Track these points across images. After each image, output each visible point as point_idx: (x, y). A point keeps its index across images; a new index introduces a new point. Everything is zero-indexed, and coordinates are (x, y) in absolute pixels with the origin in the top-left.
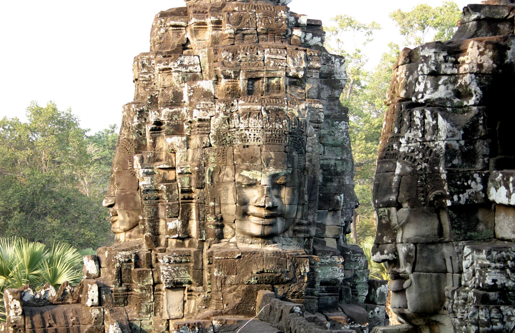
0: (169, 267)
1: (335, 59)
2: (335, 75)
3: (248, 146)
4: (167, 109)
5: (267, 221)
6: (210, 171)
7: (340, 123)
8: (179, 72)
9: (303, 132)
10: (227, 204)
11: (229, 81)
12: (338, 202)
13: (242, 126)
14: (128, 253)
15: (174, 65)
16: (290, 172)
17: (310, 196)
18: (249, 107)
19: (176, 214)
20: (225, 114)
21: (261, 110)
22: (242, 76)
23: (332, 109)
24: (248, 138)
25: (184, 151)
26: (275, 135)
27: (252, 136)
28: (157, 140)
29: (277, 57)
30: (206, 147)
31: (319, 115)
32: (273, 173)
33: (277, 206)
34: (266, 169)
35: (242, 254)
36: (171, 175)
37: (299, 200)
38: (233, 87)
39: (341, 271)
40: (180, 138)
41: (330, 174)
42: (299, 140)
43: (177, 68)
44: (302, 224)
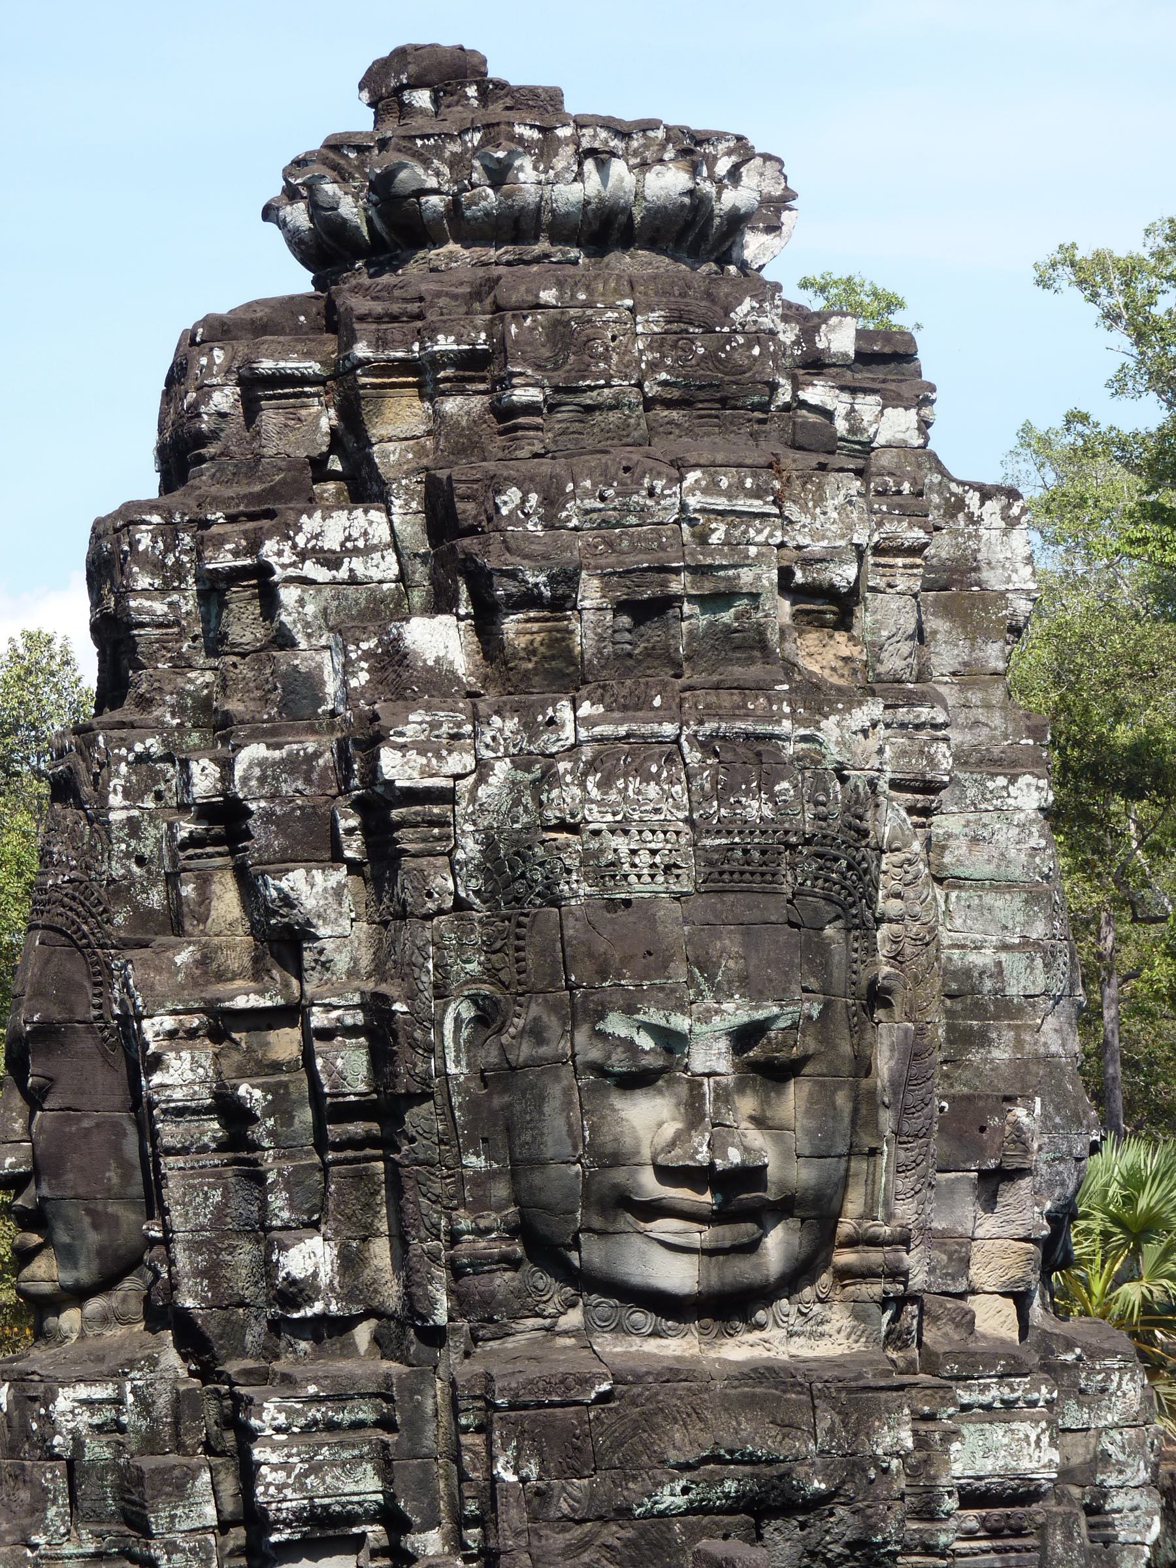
1: (982, 504)
3: (627, 903)
5: (726, 1234)
6: (458, 1020)
10: (543, 1163)
11: (528, 620)
12: (1019, 1137)
13: (598, 818)
14: (100, 1392)
15: (280, 553)
18: (622, 730)
19: (310, 1212)
20: (522, 762)
21: (677, 741)
23: (977, 723)
24: (626, 867)
25: (339, 930)
26: (746, 852)
28: (216, 888)
30: (440, 912)
32: (743, 1017)
33: (766, 1166)
34: (710, 1003)
35: (616, 1382)
37: (854, 1132)
38: (552, 643)
39: (1045, 1439)
41: (978, 1011)
42: (850, 867)
43: (293, 565)
44: (874, 1242)
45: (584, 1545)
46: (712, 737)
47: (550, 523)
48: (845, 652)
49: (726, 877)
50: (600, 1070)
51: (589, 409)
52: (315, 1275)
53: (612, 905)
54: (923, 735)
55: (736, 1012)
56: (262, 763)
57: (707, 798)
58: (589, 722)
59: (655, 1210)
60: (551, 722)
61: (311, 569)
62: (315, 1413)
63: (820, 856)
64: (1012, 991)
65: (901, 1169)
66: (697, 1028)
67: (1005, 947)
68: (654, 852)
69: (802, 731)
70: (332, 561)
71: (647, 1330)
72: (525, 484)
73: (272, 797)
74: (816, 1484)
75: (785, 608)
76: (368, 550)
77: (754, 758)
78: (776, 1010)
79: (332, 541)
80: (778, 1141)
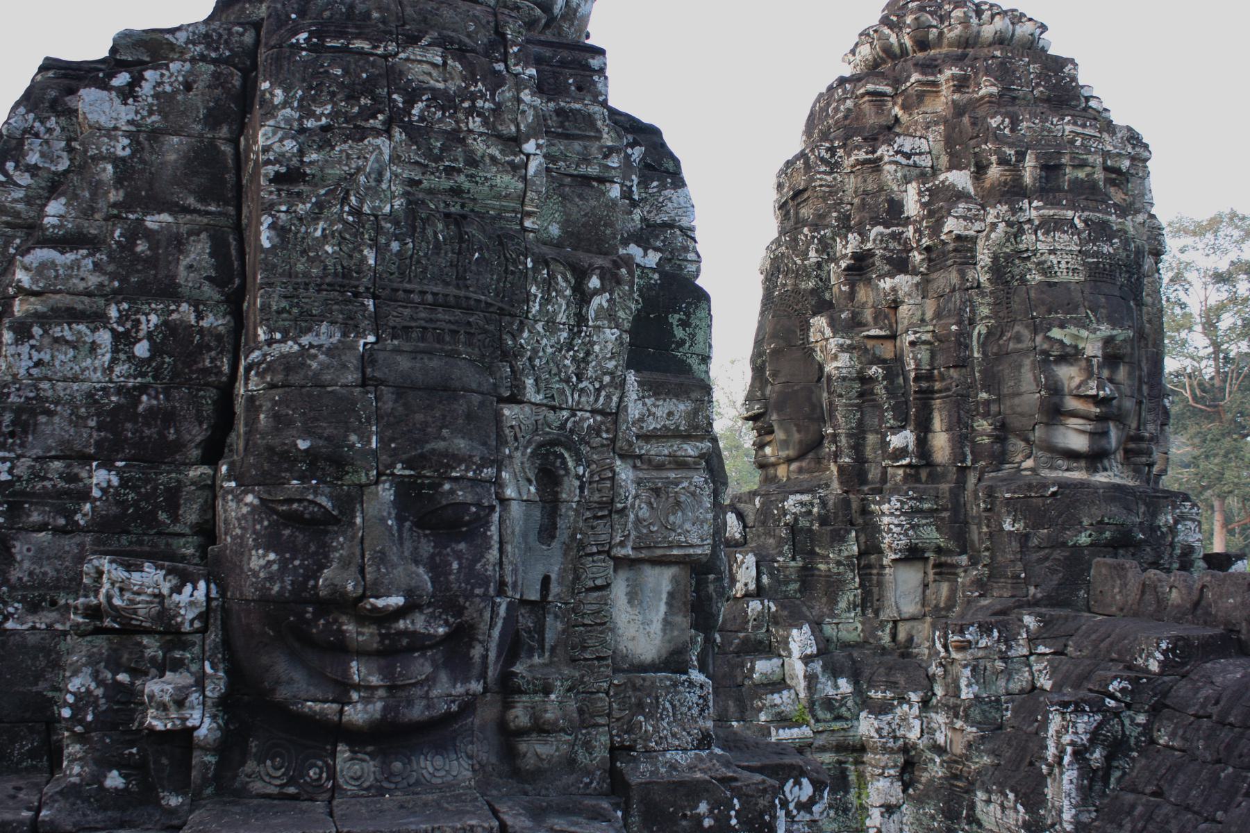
0: (902, 518)
4: (880, 229)
6: (979, 334)
8: (897, 163)
13: (1042, 247)
18: (1052, 212)
20: (1009, 224)
22: (1030, 161)
27: (1063, 265)
29: (1087, 131)
30: (972, 288)
32: (1108, 333)
36: (887, 351)
40: (908, 277)
45: (1046, 558)
47: (1012, 130)
50: (1046, 353)
51: (1014, 98)
53: (1050, 285)
55: (1105, 330)
56: (881, 234)
57: (1088, 243)
58: (1037, 208)
59: (1074, 414)
62: (911, 503)
65: (1150, 411)
70: (908, 156)
72: (1005, 115)
73: (885, 249)
76: (921, 154)
77: (1101, 231)
79: (907, 149)
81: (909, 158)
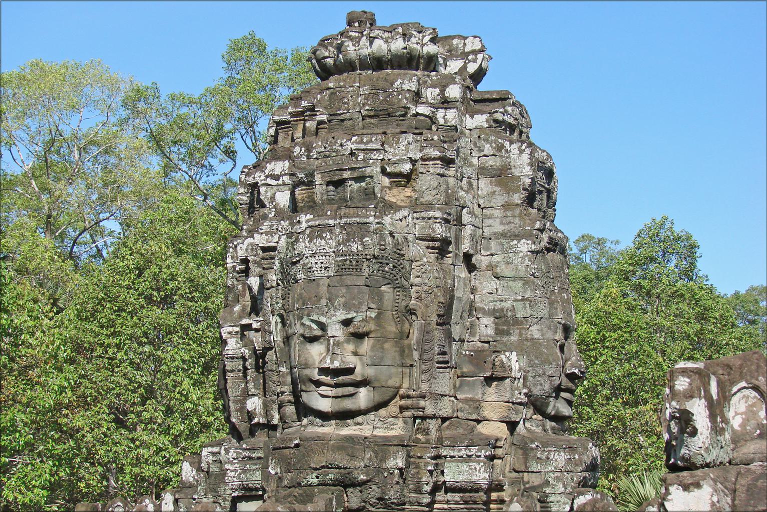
2: (513, 170)
3: (314, 280)
7: (518, 242)
9: (403, 255)
11: (304, 190)
15: (260, 177)
16: (373, 315)
17: (422, 352)
18: (317, 223)
26: (351, 262)
30: (272, 287)
31: (433, 229)
32: (343, 317)
34: (332, 312)
38: (309, 197)
39: (482, 469)
41: (506, 323)
43: (264, 180)
46: (346, 224)
47: (309, 157)
48: (409, 194)
49: (344, 270)
51: (342, 121)
52: (255, 409)
54: (431, 221)
55: (341, 315)
59: (318, 384)
60: (299, 222)
61: (269, 181)
62: (247, 454)
63: (381, 263)
64: (518, 316)
65: (423, 372)
66: (329, 321)
67: (516, 300)
68: (322, 263)
69: (376, 221)
71: (320, 424)
74: (362, 477)
75: (386, 181)
78: (355, 314)
79: (277, 172)
80: (361, 360)
81: (278, 180)
